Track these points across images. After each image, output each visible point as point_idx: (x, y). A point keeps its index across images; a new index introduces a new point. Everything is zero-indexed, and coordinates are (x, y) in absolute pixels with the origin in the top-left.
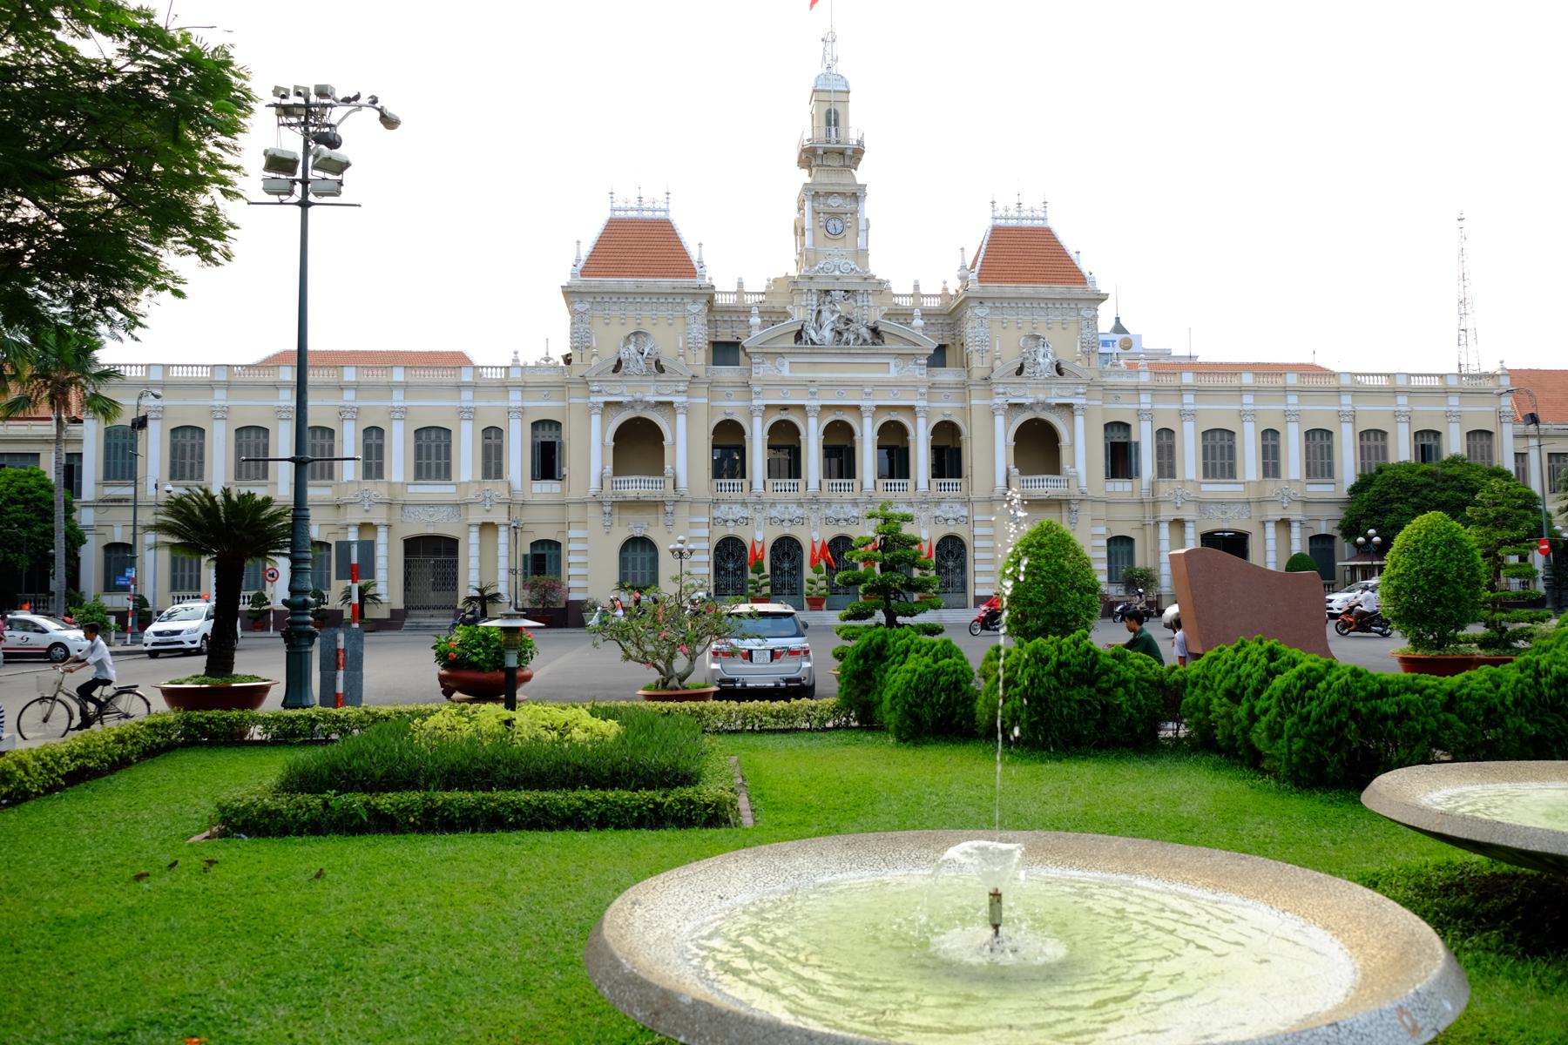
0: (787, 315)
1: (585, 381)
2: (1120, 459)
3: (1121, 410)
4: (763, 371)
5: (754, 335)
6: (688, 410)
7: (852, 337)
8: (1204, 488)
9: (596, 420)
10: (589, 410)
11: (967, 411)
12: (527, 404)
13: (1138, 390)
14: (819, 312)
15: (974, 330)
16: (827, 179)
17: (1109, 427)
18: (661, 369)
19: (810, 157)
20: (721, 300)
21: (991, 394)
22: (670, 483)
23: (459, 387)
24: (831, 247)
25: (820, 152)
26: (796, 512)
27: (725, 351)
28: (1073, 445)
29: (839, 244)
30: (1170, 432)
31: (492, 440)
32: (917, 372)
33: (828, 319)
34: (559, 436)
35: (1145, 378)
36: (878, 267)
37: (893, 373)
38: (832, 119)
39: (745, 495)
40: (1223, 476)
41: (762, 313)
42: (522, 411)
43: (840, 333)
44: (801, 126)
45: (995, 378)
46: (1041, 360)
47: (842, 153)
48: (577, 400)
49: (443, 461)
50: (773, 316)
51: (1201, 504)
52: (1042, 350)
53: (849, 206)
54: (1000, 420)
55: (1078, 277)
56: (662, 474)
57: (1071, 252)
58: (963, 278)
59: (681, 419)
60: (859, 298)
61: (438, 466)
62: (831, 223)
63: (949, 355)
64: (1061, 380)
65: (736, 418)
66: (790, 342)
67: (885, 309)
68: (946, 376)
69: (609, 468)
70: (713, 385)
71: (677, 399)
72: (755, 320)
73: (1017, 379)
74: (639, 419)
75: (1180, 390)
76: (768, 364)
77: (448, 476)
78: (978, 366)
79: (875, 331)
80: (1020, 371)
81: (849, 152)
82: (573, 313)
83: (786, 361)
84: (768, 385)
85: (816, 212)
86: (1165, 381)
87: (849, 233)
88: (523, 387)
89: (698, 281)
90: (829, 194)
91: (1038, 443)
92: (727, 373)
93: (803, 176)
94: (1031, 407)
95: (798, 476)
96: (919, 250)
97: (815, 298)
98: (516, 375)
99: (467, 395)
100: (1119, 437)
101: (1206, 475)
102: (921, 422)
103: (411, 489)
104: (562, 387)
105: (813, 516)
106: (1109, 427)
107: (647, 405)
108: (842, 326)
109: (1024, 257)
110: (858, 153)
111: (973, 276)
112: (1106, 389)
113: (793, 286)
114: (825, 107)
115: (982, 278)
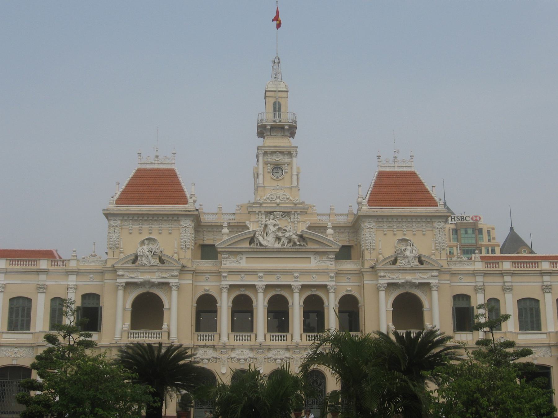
0: (247, 227)
1: (114, 270)
3: (464, 286)
4: (229, 264)
5: (223, 239)
6: (179, 288)
7: (286, 241)
8: (520, 337)
9: (121, 293)
10: (117, 289)
11: (362, 287)
12: (78, 283)
13: (474, 274)
14: (266, 226)
16: (273, 142)
17: (457, 298)
18: (162, 261)
19: (263, 131)
20: (206, 219)
21: (378, 277)
22: (165, 336)
23: (39, 272)
24: (274, 184)
25: (269, 127)
26: (247, 354)
28: (431, 310)
29: (280, 184)
30: (497, 301)
31: (58, 306)
32: (329, 264)
33: (272, 228)
34: (99, 304)
36: (305, 196)
37: (314, 263)
38: (277, 108)
39: (215, 343)
40: (533, 329)
41: (230, 226)
42: (76, 288)
43: (278, 239)
44: (260, 111)
45: (379, 267)
46: (408, 253)
47: (282, 128)
49: (25, 319)
50: (237, 227)
52: (409, 248)
53: (286, 159)
54: (382, 294)
55: (432, 202)
56: (161, 329)
57: (429, 187)
58: (359, 203)
59: (174, 293)
60: (292, 217)
61: (22, 321)
62: (275, 171)
63: (354, 253)
64: (422, 266)
65: (213, 293)
66: (246, 245)
67: (308, 223)
68: (348, 266)
69: (128, 323)
70: (195, 273)
71: (172, 281)
72: (225, 230)
73: (393, 267)
74: (148, 293)
75: (502, 274)
76: (232, 258)
77: (28, 327)
78: (369, 258)
79: (301, 237)
80: (395, 262)
81: (287, 127)
82: (110, 225)
83: (244, 257)
84: (232, 272)
85: (266, 164)
86: (491, 268)
87: (287, 177)
88: (78, 273)
89: (190, 207)
90: (273, 153)
92: (206, 265)
93: (260, 141)
94: (403, 285)
95: (252, 331)
97: (264, 217)
98: (73, 265)
99: (43, 277)
100: (462, 304)
101: (521, 329)
102: (332, 296)
103: (5, 336)
104: (102, 272)
105: (259, 356)
106: (457, 298)
107: (153, 285)
108: (280, 234)
109: (399, 190)
111: (365, 202)
113: (251, 209)
114: (272, 101)
115: (370, 203)
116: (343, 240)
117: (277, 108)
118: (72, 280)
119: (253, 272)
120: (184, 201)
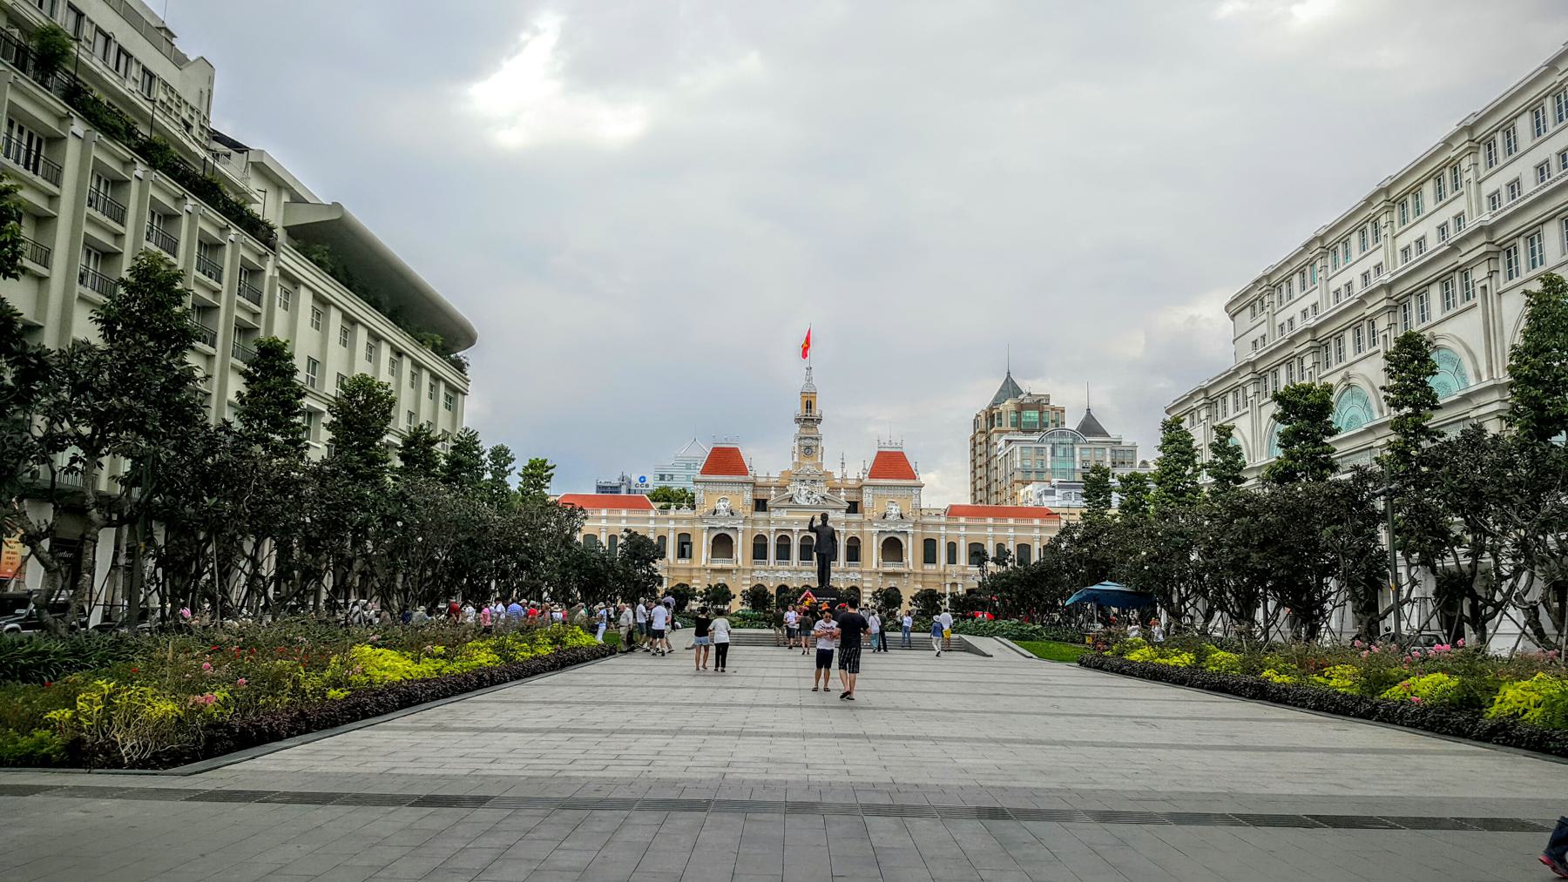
1: (701, 519)
2: (930, 555)
3: (931, 533)
4: (775, 514)
13: (939, 525)
15: (867, 499)
20: (760, 481)
24: (807, 461)
27: (761, 505)
33: (804, 492)
35: (943, 520)
38: (809, 405)
48: (698, 525)
50: (783, 488)
51: (965, 576)
68: (854, 517)
70: (754, 522)
75: (959, 526)
84: (778, 521)
88: (675, 519)
89: (750, 477)
91: (892, 548)
92: (760, 515)
96: (846, 459)
110: (819, 421)
112: (924, 525)
115: (871, 477)
116: (853, 497)
117: (809, 405)
118: (672, 524)
119: (791, 521)
120: (746, 473)
